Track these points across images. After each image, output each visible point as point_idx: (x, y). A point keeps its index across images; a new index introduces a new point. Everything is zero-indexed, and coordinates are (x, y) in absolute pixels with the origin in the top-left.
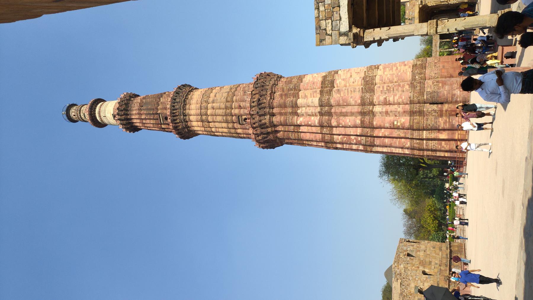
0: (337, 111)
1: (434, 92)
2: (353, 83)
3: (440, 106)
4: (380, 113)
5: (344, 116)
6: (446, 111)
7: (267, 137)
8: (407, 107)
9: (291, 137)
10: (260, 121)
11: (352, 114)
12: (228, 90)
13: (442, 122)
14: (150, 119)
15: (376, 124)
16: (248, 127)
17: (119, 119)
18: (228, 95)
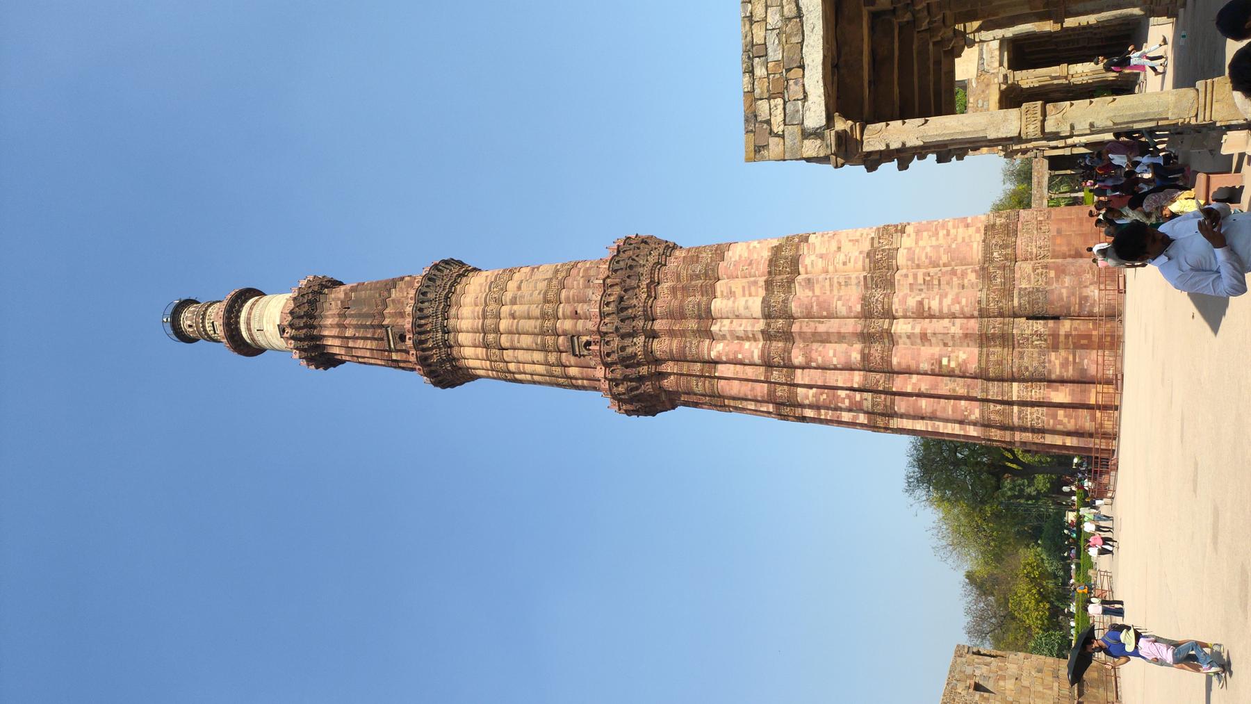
0: (805, 329)
1: (1038, 290)
2: (844, 264)
3: (1051, 323)
4: (909, 337)
5: (822, 342)
6: (1067, 336)
8: (973, 325)
9: (696, 389)
10: (623, 349)
11: (841, 338)
12: (549, 275)
13: (1056, 363)
14: (365, 338)
15: (899, 363)
16: (592, 363)
17: (292, 338)
18: (549, 285)
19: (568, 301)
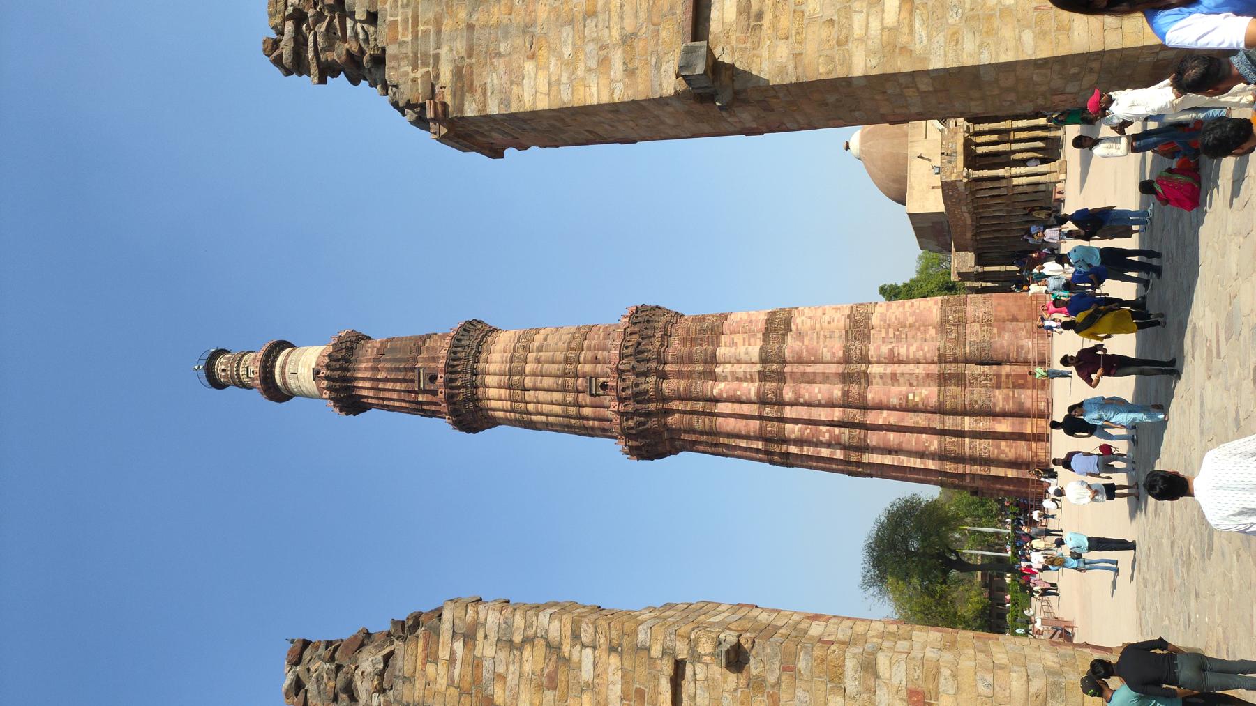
3: (995, 367)
4: (881, 377)
5: (809, 382)
6: (1008, 376)
7: (644, 424)
8: (934, 369)
10: (637, 385)
11: (825, 378)
12: (573, 330)
13: (1000, 398)
14: (395, 381)
16: (606, 403)
17: (327, 378)
18: (573, 337)
19: (589, 349)
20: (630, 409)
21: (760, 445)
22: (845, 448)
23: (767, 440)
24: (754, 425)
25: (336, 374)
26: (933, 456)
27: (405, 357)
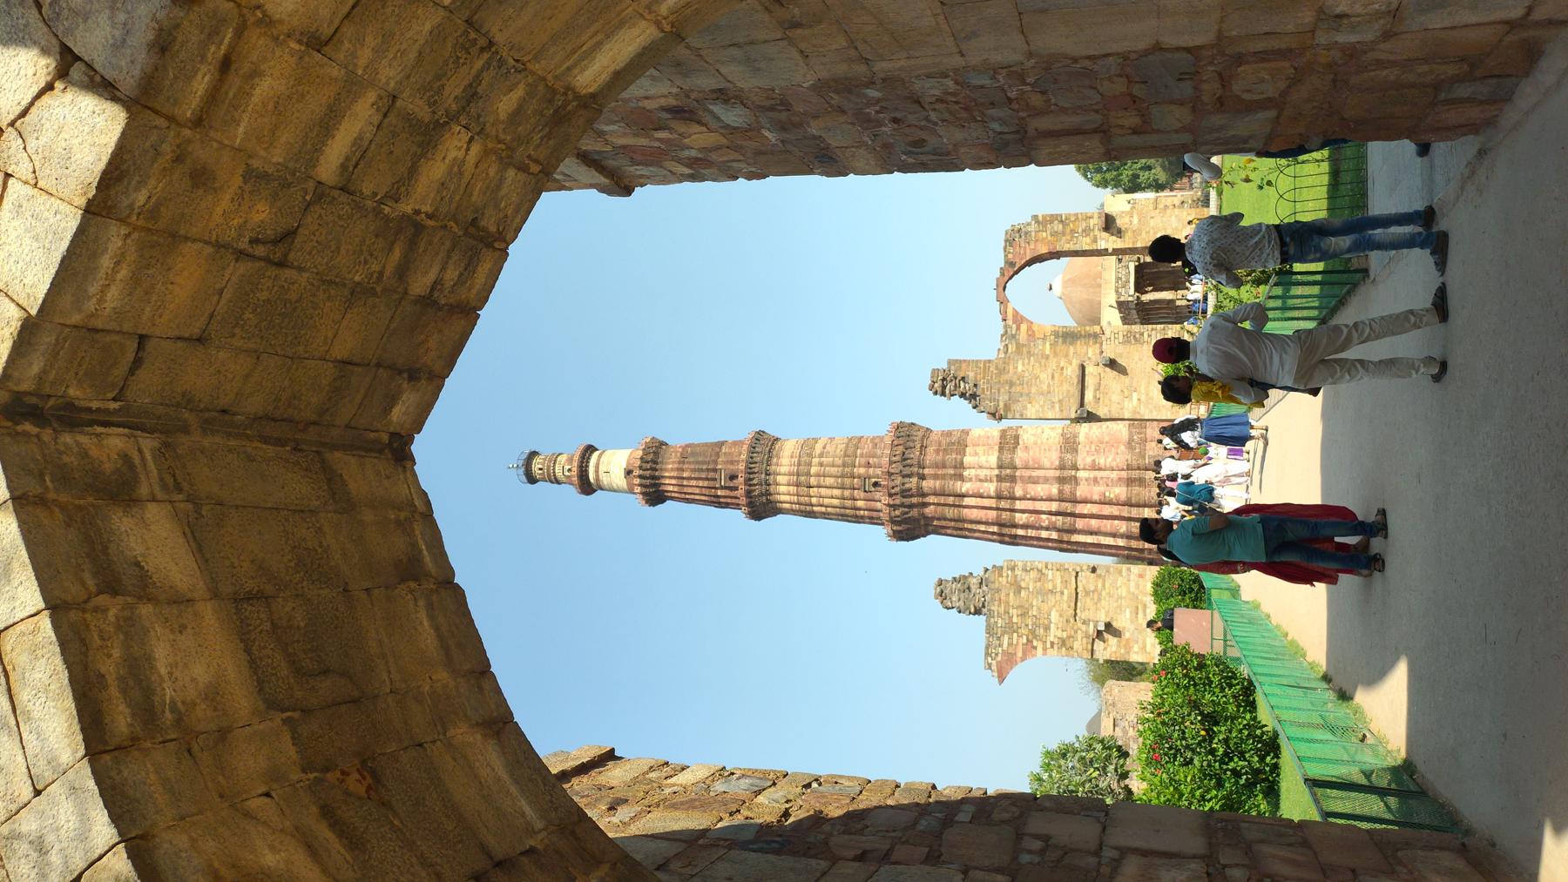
8: (1124, 474)
11: (1046, 480)
17: (640, 477)
20: (898, 502)
21: (995, 529)
22: (1059, 530)
23: (1001, 525)
24: (992, 514)
25: (648, 473)
26: (1122, 536)
27: (705, 458)
